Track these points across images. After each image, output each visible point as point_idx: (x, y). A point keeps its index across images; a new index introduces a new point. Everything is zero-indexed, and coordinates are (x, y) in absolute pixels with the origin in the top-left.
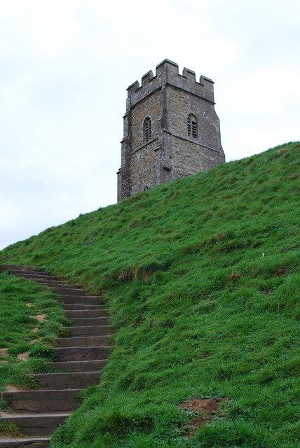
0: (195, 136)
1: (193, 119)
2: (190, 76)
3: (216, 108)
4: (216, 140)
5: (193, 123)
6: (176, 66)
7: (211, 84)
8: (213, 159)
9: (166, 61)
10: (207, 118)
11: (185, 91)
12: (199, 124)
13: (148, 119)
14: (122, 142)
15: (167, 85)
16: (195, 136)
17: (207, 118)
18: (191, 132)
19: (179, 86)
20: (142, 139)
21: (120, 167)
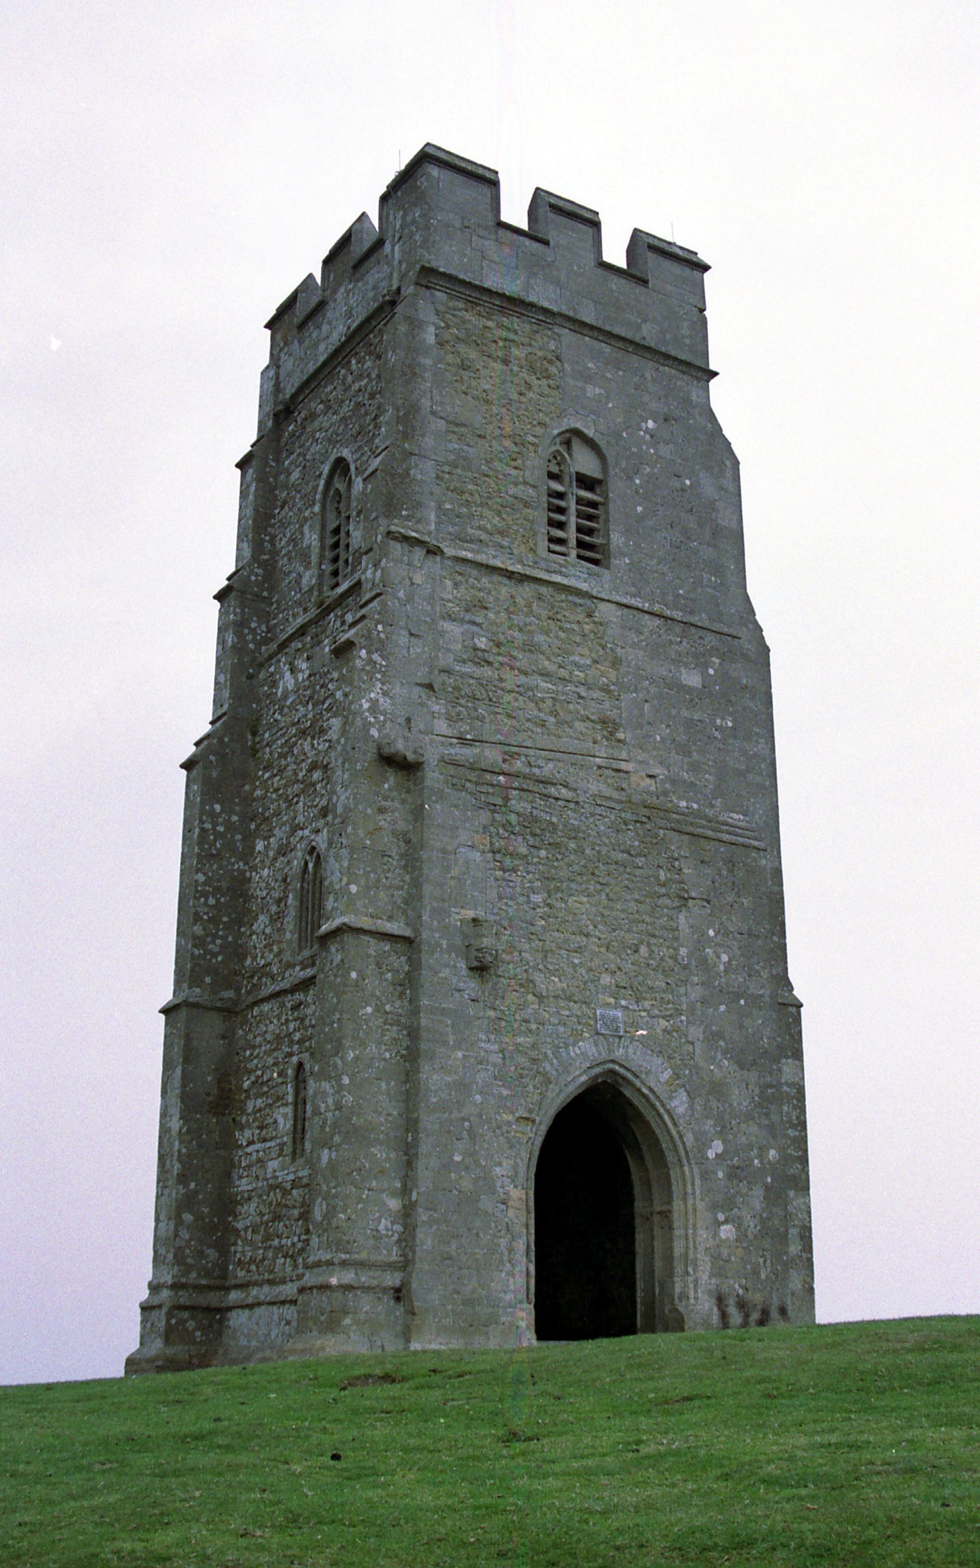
0: (592, 552)
1: (584, 462)
2: (561, 233)
3: (720, 396)
4: (718, 570)
5: (585, 482)
6: (487, 180)
8: (692, 679)
9: (428, 158)
12: (617, 488)
13: (341, 466)
14: (220, 597)
15: (429, 276)
16: (592, 552)
17: (666, 451)
18: (571, 534)
20: (309, 578)
21: (205, 728)
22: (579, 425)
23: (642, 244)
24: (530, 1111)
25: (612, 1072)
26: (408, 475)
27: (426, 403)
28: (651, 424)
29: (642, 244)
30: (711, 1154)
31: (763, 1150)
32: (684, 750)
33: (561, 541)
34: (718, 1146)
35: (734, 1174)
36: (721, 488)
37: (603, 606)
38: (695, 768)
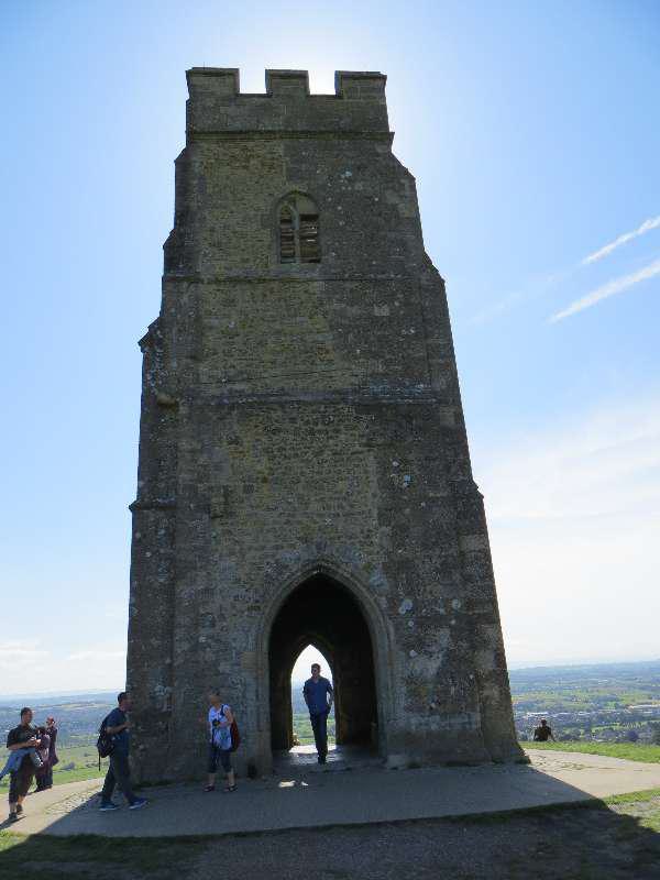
1: (306, 207)
4: (403, 244)
6: (232, 75)
7: (380, 82)
8: (383, 311)
10: (359, 186)
11: (260, 132)
17: (359, 186)
19: (238, 125)
22: (296, 187)
23: (342, 78)
24: (257, 601)
25: (320, 567)
26: (183, 245)
27: (194, 205)
28: (348, 174)
29: (342, 78)
30: (402, 610)
31: (447, 602)
32: (376, 356)
33: (293, 256)
34: (407, 604)
35: (422, 623)
36: (401, 197)
37: (315, 284)
38: (387, 363)
